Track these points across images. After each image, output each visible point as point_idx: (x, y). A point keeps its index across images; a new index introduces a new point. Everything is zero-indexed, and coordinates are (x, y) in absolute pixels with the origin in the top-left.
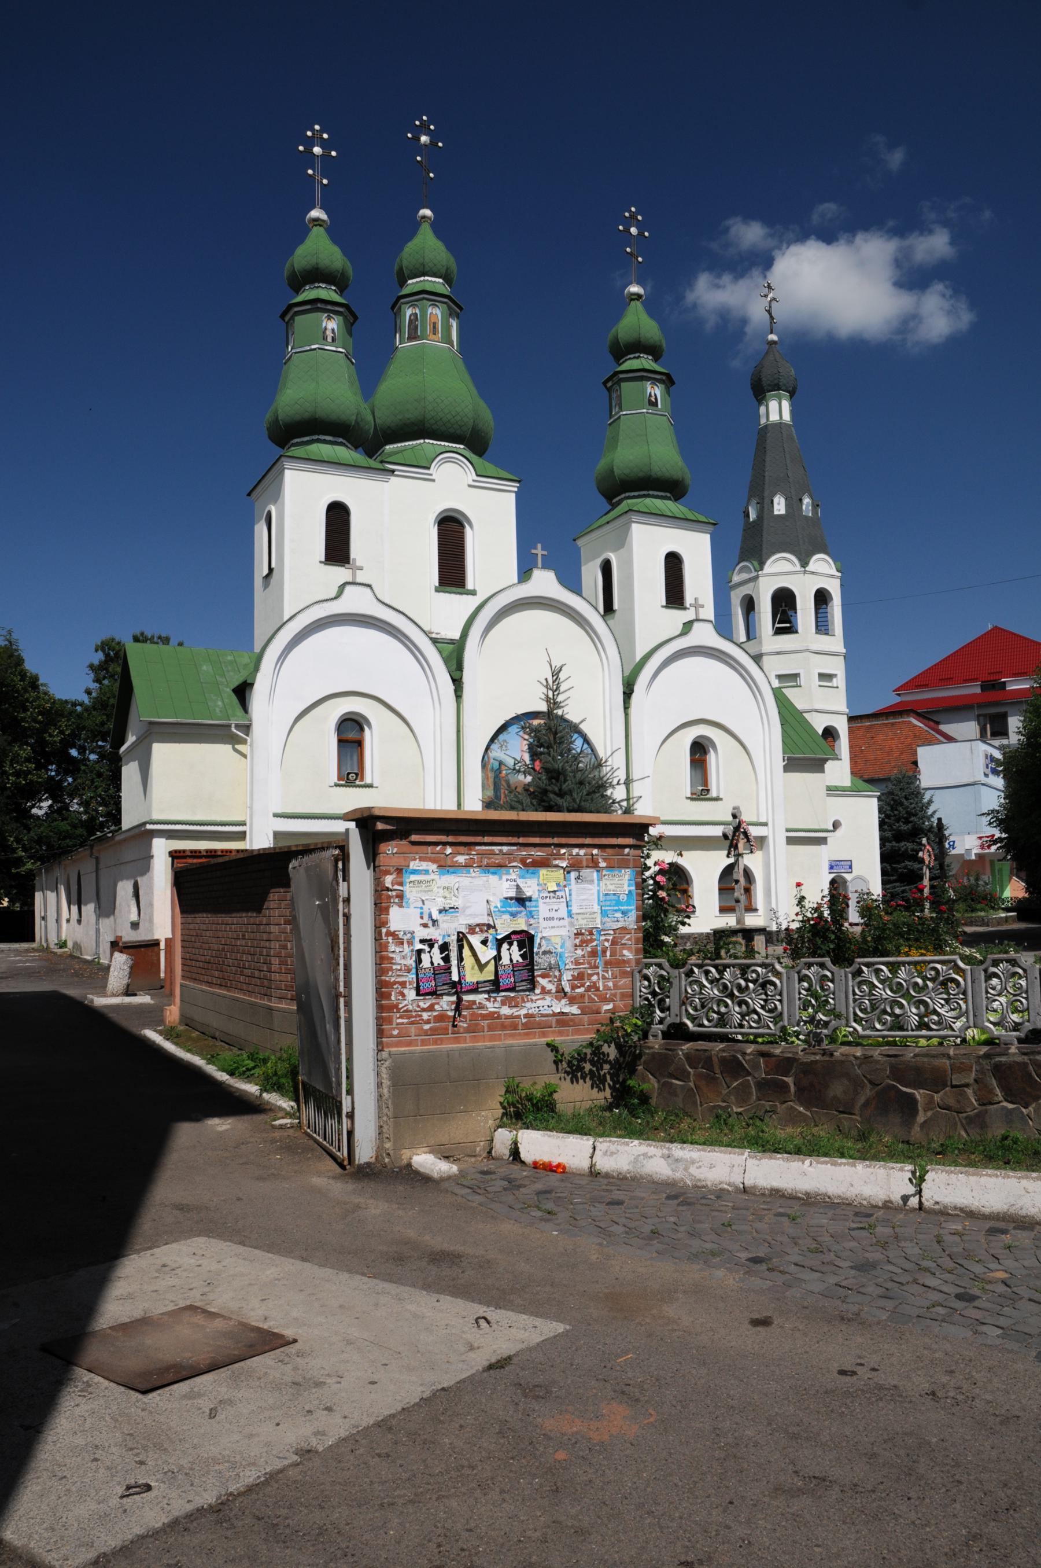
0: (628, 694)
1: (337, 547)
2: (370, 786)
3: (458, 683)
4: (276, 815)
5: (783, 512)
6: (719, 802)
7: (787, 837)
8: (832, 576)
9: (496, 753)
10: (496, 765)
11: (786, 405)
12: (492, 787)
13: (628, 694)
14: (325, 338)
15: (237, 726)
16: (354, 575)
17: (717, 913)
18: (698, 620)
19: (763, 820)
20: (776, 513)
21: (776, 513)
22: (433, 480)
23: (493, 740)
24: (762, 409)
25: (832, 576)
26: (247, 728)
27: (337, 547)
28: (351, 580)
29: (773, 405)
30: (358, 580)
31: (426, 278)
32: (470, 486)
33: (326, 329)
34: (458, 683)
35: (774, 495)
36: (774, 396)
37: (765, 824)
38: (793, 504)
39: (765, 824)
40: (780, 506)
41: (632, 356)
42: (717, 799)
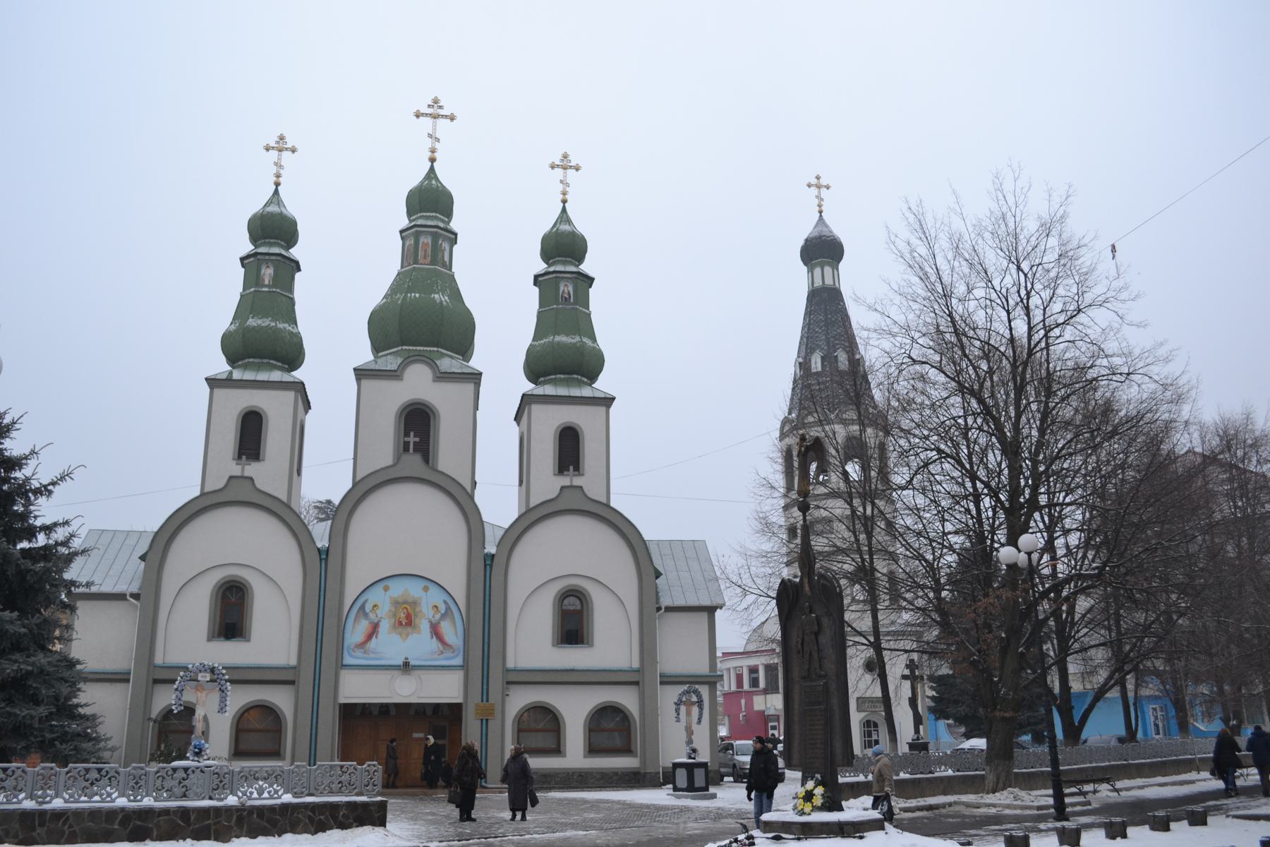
5: (819, 369)
11: (828, 270)
16: (243, 470)
28: (239, 474)
29: (818, 271)
30: (246, 474)
38: (828, 359)
40: (816, 364)
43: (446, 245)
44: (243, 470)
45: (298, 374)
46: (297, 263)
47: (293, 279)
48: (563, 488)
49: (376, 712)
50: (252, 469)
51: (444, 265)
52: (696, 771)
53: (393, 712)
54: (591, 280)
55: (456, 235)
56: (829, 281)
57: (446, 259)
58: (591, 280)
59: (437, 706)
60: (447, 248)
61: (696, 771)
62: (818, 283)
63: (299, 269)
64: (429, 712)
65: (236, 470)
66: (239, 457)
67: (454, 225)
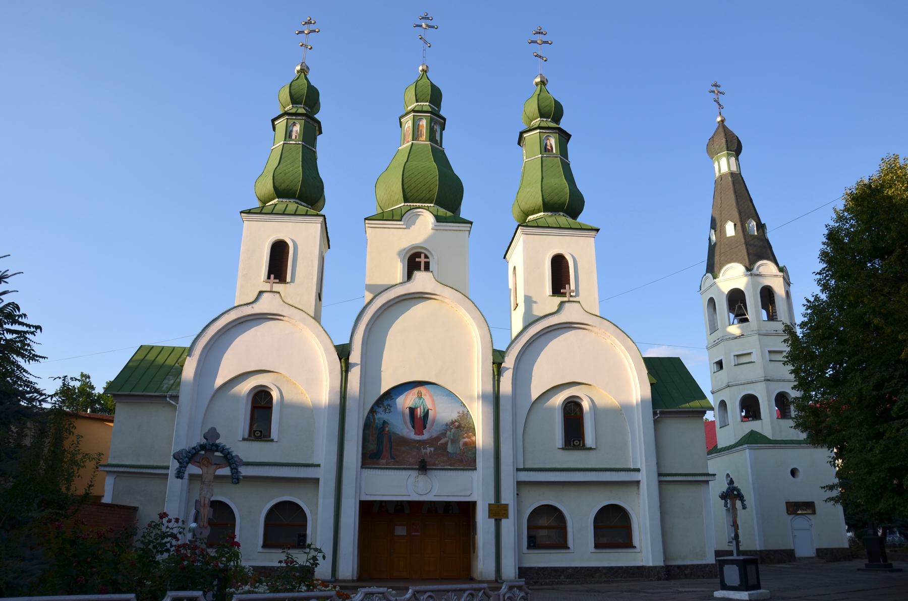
6: (592, 452)
7: (660, 482)
8: (776, 276)
9: (381, 416)
10: (380, 425)
14: (290, 136)
15: (172, 397)
16: (272, 287)
17: (594, 550)
18: (569, 301)
20: (728, 235)
21: (728, 235)
24: (716, 165)
25: (776, 276)
26: (176, 398)
30: (274, 290)
33: (292, 131)
35: (726, 222)
36: (723, 155)
37: (638, 470)
38: (742, 226)
40: (730, 229)
43: (437, 128)
44: (272, 287)
45: (322, 212)
46: (319, 123)
47: (315, 139)
48: (562, 303)
50: (278, 287)
51: (436, 142)
52: (748, 567)
54: (569, 136)
55: (445, 119)
56: (734, 168)
57: (438, 138)
58: (569, 136)
59: (448, 504)
60: (439, 130)
61: (748, 567)
62: (725, 169)
63: (321, 133)
65: (267, 287)
66: (269, 278)
67: (442, 113)
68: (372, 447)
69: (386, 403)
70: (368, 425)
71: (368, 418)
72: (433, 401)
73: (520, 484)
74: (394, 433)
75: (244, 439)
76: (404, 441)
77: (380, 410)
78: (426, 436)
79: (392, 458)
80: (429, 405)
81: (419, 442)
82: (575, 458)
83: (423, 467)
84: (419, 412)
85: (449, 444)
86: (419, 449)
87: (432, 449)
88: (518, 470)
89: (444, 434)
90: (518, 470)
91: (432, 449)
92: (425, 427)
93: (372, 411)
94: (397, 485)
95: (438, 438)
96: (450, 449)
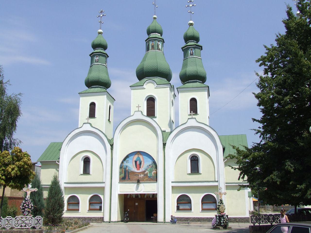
0: (164, 145)
1: (92, 114)
2: (91, 175)
3: (112, 146)
4: (65, 183)
9: (125, 164)
10: (125, 167)
12: (124, 174)
13: (164, 145)
15: (58, 162)
18: (192, 118)
19: (216, 180)
22: (145, 88)
23: (125, 159)
27: (92, 114)
30: (89, 122)
31: (156, 34)
32: (155, 88)
34: (112, 146)
39: (217, 181)
41: (191, 41)
42: (201, 174)
46: (106, 54)
48: (188, 119)
49: (134, 197)
50: (91, 120)
53: (140, 197)
64: (151, 197)
68: (123, 175)
69: (127, 159)
70: (121, 167)
71: (121, 165)
72: (143, 158)
73: (173, 187)
74: (130, 170)
75: (81, 175)
76: (133, 173)
77: (125, 162)
78: (141, 170)
79: (129, 179)
80: (142, 159)
81: (138, 173)
82: (195, 177)
83: (138, 182)
84: (138, 162)
85: (149, 173)
86: (138, 175)
87: (143, 175)
88: (172, 182)
89: (147, 170)
90: (172, 182)
91: (143, 175)
92: (140, 167)
93: (122, 162)
94: (131, 189)
95: (145, 171)
96: (149, 175)
